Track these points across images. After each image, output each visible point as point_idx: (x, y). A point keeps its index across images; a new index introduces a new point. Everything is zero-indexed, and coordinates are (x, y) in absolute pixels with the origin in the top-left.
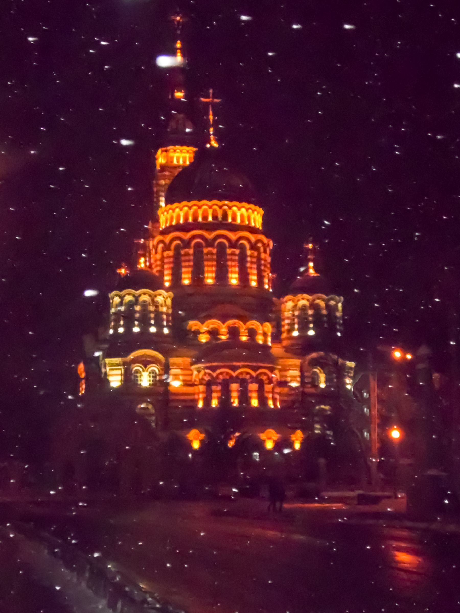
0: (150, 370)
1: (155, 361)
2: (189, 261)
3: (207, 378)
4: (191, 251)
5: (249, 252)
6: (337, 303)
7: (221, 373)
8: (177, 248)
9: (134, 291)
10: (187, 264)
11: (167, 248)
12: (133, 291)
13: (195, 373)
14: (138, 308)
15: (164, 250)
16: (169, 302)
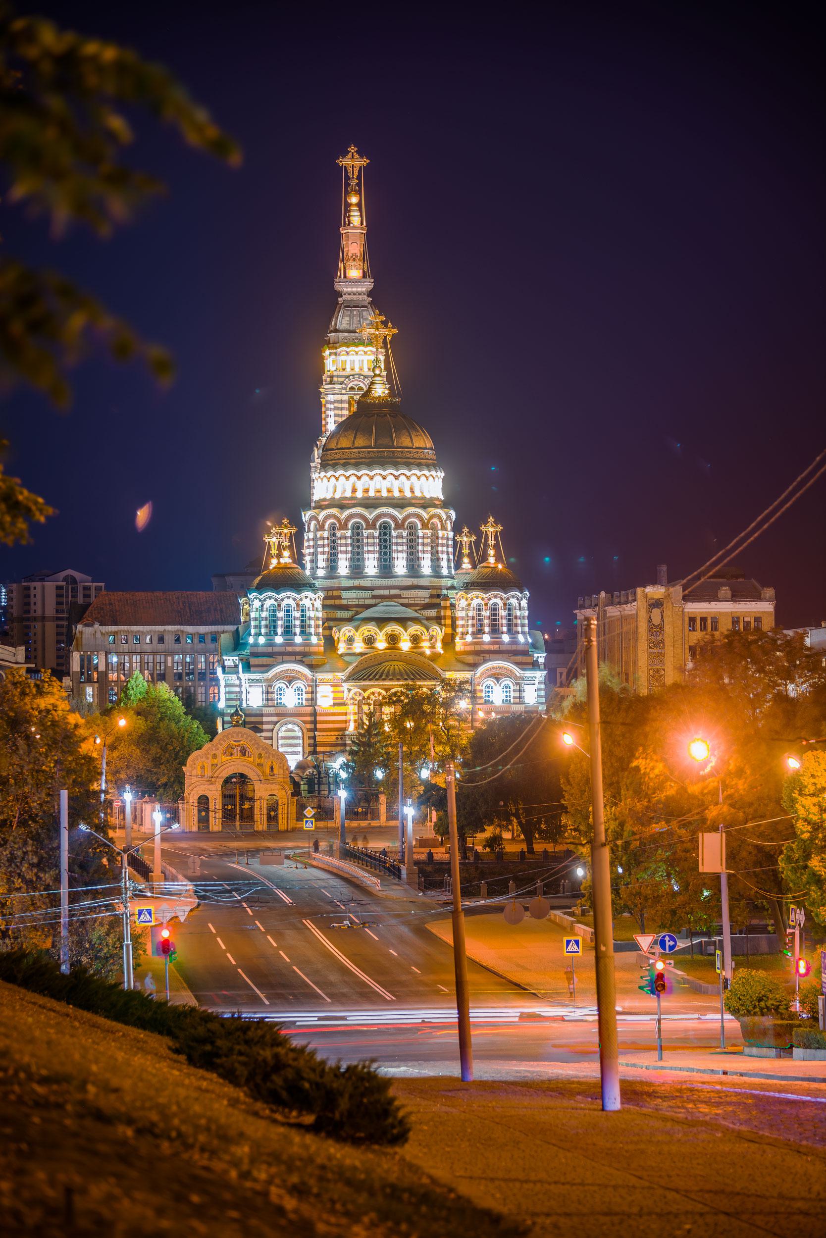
0: (295, 687)
2: (346, 545)
3: (358, 698)
4: (349, 534)
7: (373, 694)
8: (333, 528)
10: (343, 549)
11: (321, 527)
14: (280, 614)
15: (317, 530)
16: (318, 604)
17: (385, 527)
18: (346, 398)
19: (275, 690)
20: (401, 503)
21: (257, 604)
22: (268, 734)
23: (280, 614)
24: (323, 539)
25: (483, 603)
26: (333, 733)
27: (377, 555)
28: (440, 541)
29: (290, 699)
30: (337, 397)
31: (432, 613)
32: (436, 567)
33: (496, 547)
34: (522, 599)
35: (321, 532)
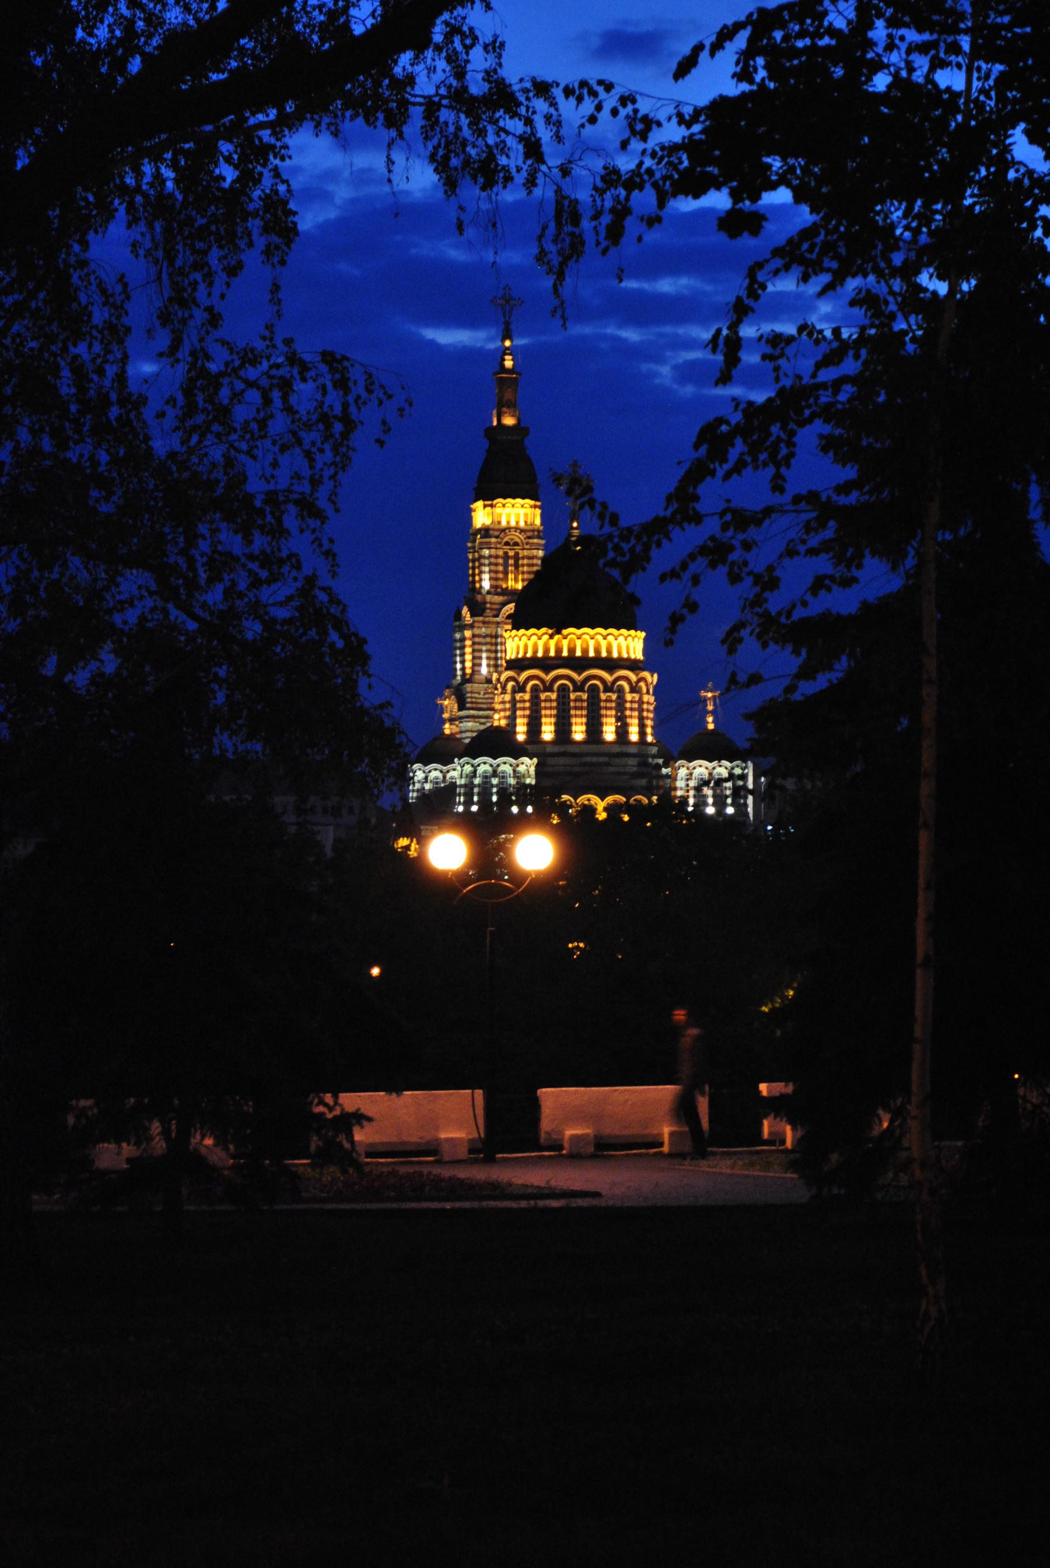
2: (551, 708)
4: (554, 696)
5: (629, 697)
8: (535, 689)
9: (490, 759)
10: (548, 712)
12: (489, 760)
15: (514, 691)
16: (532, 770)
18: (501, 553)
20: (611, 664)
21: (468, 769)
24: (524, 701)
25: (706, 772)
27: (584, 720)
30: (493, 551)
31: (643, 782)
32: (642, 733)
33: (713, 713)
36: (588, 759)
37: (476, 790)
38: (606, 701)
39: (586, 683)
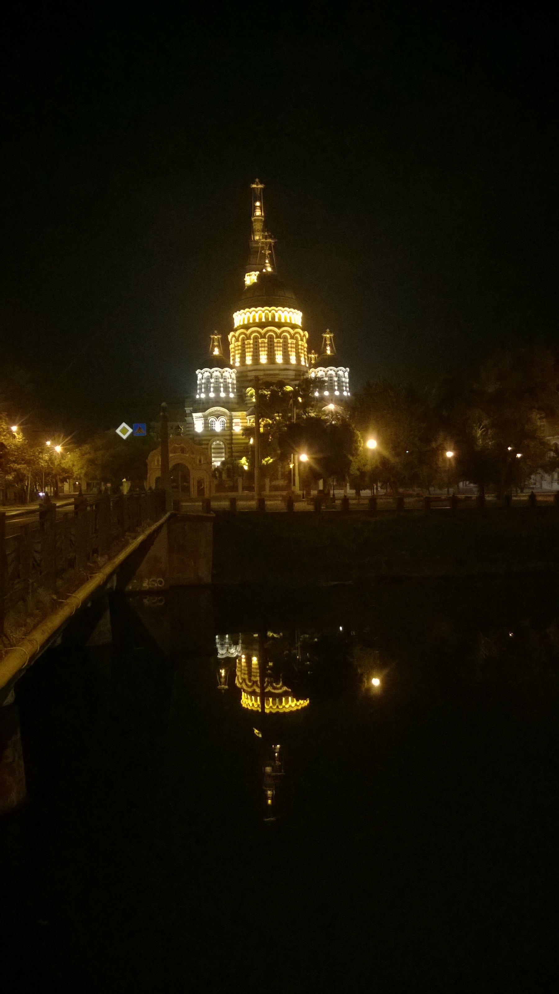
1: (223, 414)
2: (250, 348)
4: (251, 341)
5: (290, 341)
6: (344, 372)
8: (243, 340)
10: (249, 350)
11: (237, 340)
13: (248, 421)
14: (212, 380)
16: (234, 376)
17: (271, 338)
19: (210, 422)
22: (205, 446)
23: (212, 380)
25: (324, 373)
26: (242, 445)
27: (266, 353)
28: (300, 347)
29: (218, 427)
33: (331, 345)
34: (345, 372)
35: (237, 343)
36: (269, 372)
37: (203, 386)
38: (277, 343)
39: (267, 334)
